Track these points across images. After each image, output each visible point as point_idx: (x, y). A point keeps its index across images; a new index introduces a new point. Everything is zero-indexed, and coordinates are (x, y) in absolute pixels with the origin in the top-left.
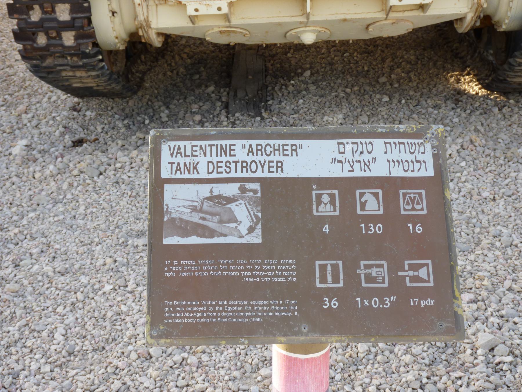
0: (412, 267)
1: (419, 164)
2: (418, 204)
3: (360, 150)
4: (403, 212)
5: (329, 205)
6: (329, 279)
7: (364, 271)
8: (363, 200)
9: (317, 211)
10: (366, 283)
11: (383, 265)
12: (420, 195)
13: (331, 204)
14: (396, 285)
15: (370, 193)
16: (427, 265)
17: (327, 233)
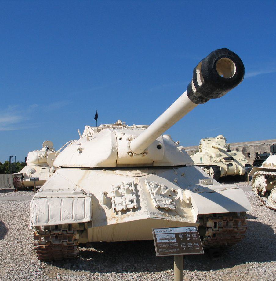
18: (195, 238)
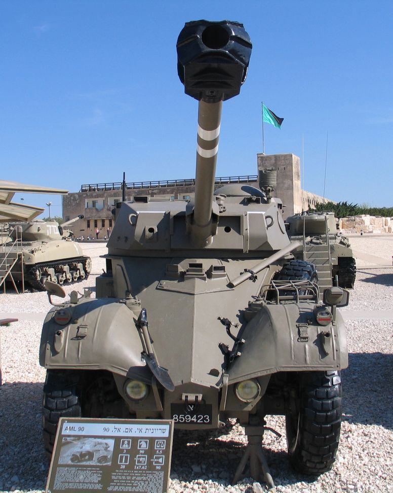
0: (156, 458)
6: (124, 461)
8: (141, 444)
9: (122, 447)
12: (164, 442)
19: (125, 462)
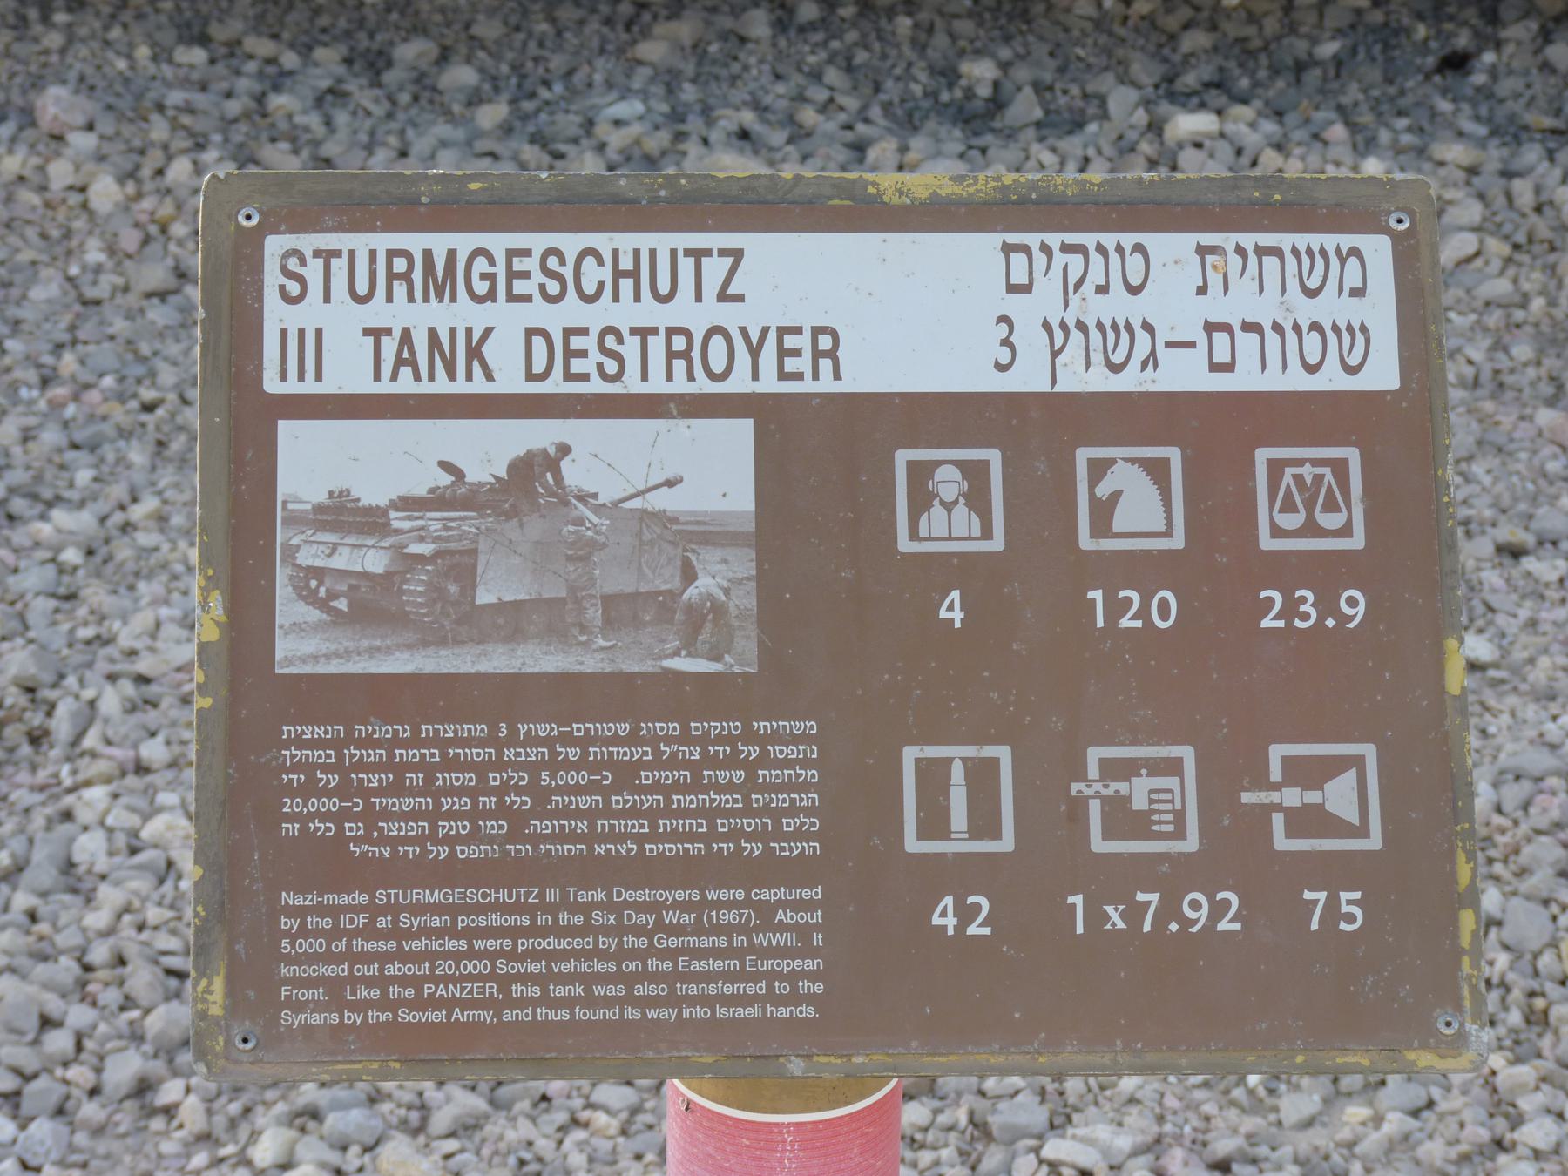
1: (1255, 337)
2: (1330, 506)
3: (1096, 276)
4: (1267, 543)
5: (961, 511)
6: (959, 818)
7: (1098, 786)
8: (1103, 490)
9: (914, 535)
10: (1107, 835)
11: (1180, 760)
12: (1340, 467)
13: (971, 506)
14: (1235, 848)
15: (1133, 461)
16: (1358, 762)
17: (958, 625)
18: (1328, 573)
19: (975, 833)
